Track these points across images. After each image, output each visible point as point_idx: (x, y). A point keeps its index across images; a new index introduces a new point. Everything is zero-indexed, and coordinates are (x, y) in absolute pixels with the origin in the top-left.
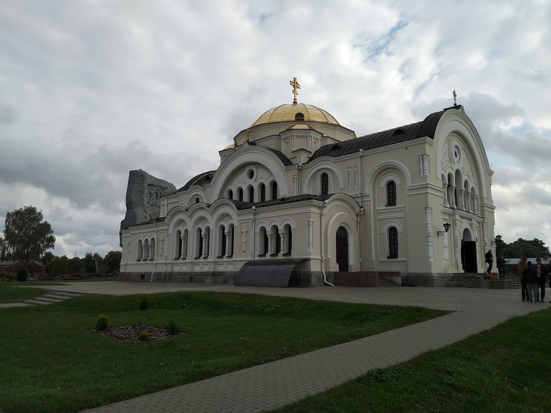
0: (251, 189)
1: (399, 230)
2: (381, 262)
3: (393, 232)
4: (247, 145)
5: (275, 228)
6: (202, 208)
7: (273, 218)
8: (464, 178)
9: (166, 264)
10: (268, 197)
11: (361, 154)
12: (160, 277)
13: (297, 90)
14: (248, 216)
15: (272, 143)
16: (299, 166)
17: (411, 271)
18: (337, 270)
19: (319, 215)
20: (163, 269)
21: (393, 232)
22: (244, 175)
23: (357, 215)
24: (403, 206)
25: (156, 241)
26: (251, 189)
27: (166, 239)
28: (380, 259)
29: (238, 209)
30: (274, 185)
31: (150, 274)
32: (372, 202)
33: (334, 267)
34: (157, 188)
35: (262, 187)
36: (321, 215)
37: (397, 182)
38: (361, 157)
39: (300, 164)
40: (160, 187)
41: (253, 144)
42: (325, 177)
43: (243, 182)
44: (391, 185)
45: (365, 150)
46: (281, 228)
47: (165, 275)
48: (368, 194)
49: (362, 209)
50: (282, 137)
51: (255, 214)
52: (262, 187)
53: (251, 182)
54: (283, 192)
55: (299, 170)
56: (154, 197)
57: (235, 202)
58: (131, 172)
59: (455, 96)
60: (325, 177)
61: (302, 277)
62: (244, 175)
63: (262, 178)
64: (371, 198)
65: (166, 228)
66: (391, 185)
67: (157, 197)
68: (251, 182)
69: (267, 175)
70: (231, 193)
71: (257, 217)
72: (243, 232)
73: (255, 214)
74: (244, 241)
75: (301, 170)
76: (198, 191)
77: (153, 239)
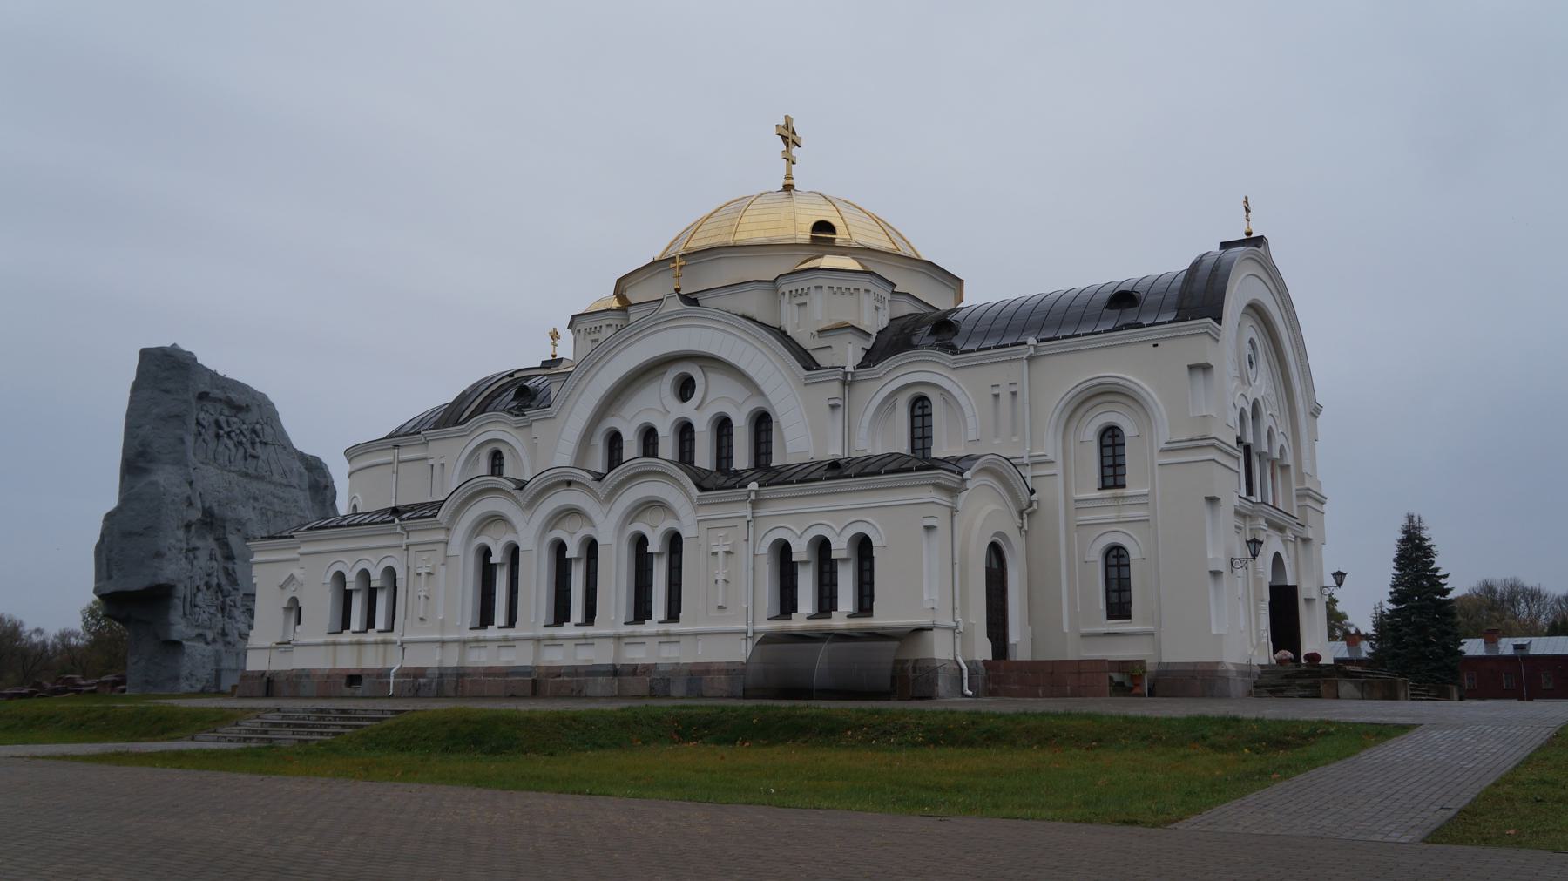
0: (685, 430)
1: (1134, 553)
2: (1084, 636)
3: (1116, 558)
4: (676, 305)
5: (822, 546)
6: (569, 483)
8: (1266, 422)
9: (443, 642)
10: (742, 458)
11: (1032, 350)
12: (422, 680)
13: (795, 151)
14: (732, 509)
15: (753, 303)
16: (846, 373)
17: (1165, 660)
18: (990, 657)
19: (948, 511)
20: (430, 659)
21: (1116, 558)
22: (664, 386)
23: (1021, 513)
24: (1145, 491)
25: (401, 575)
26: (685, 430)
27: (441, 572)
28: (1084, 630)
29: (701, 488)
30: (762, 422)
31: (383, 674)
32: (1060, 479)
33: (983, 650)
34: (219, 406)
35: (723, 426)
36: (953, 511)
37: (1129, 429)
38: (1030, 359)
39: (850, 369)
40: (230, 403)
41: (690, 300)
42: (920, 407)
43: (657, 407)
44: (1111, 438)
45: (1043, 341)
46: (840, 547)
47: (441, 675)
48: (1050, 457)
49: (1034, 497)
50: (785, 289)
51: (755, 504)
52: (723, 426)
53: (688, 410)
54: (797, 442)
55: (844, 383)
56: (209, 436)
58: (146, 354)
59: (1247, 211)
60: (920, 407)
61: (911, 675)
62: (664, 386)
63: (717, 398)
64: (1057, 469)
65: (441, 536)
66: (1111, 438)
67: (218, 436)
68: (688, 410)
70: (615, 439)
71: (760, 512)
72: (715, 554)
73: (755, 504)
74: (720, 578)
75: (852, 383)
76: (498, 429)
77: (390, 573)
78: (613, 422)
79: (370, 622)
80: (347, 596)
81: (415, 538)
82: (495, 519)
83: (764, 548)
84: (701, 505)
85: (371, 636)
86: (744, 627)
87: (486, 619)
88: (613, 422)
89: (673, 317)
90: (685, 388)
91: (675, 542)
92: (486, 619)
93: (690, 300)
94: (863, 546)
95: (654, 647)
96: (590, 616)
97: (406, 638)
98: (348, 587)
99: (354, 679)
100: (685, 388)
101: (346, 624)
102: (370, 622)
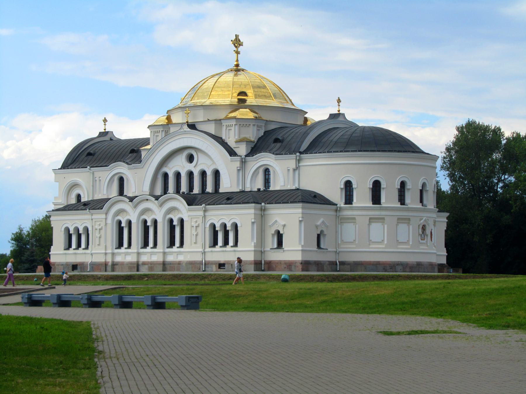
0: (191, 174)
5: (225, 226)
6: (147, 200)
7: (222, 215)
14: (197, 211)
16: (242, 159)
20: (100, 259)
26: (191, 174)
30: (217, 174)
35: (203, 174)
39: (243, 157)
43: (180, 165)
52: (203, 174)
53: (190, 167)
57: (183, 196)
68: (190, 167)
69: (209, 162)
71: (207, 214)
72: (193, 226)
78: (165, 169)
79: (79, 245)
80: (70, 236)
81: (94, 216)
82: (121, 211)
83: (208, 225)
84: (189, 210)
85: (80, 251)
86: (201, 250)
87: (120, 245)
88: (165, 169)
89: (185, 133)
90: (191, 159)
91: (182, 221)
92: (120, 245)
93: (192, 126)
94: (236, 227)
95: (176, 255)
96: (155, 245)
97: (93, 252)
98: (71, 233)
99: (75, 267)
100: (191, 159)
101: (70, 246)
102: (79, 245)
